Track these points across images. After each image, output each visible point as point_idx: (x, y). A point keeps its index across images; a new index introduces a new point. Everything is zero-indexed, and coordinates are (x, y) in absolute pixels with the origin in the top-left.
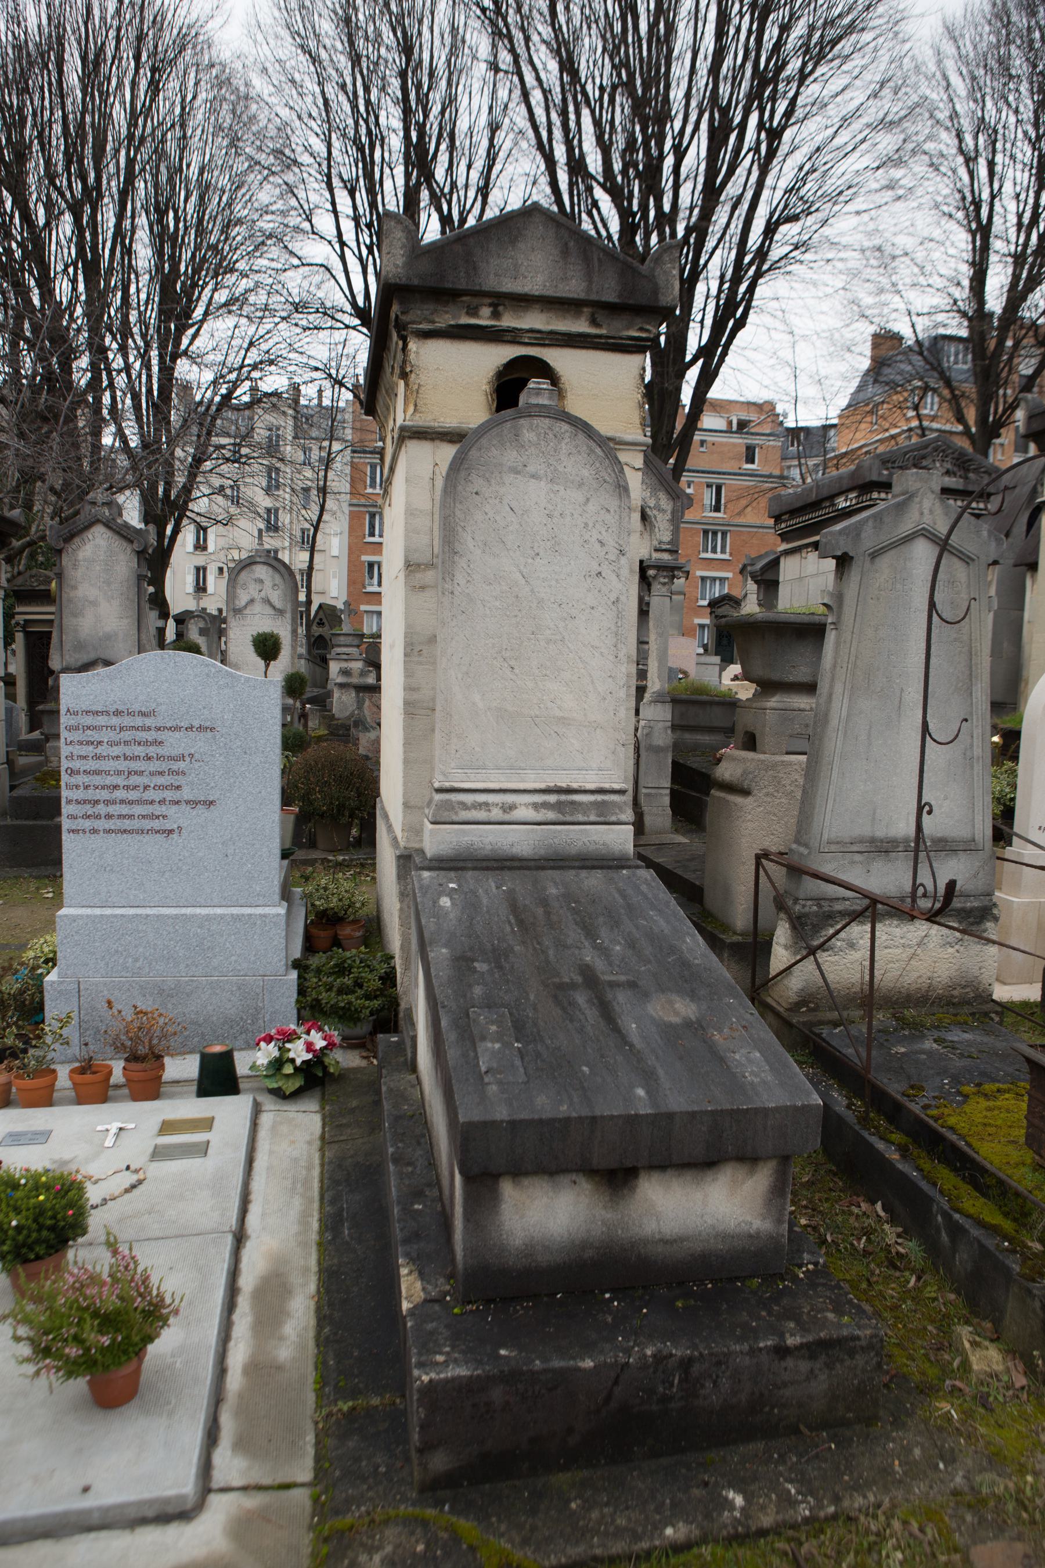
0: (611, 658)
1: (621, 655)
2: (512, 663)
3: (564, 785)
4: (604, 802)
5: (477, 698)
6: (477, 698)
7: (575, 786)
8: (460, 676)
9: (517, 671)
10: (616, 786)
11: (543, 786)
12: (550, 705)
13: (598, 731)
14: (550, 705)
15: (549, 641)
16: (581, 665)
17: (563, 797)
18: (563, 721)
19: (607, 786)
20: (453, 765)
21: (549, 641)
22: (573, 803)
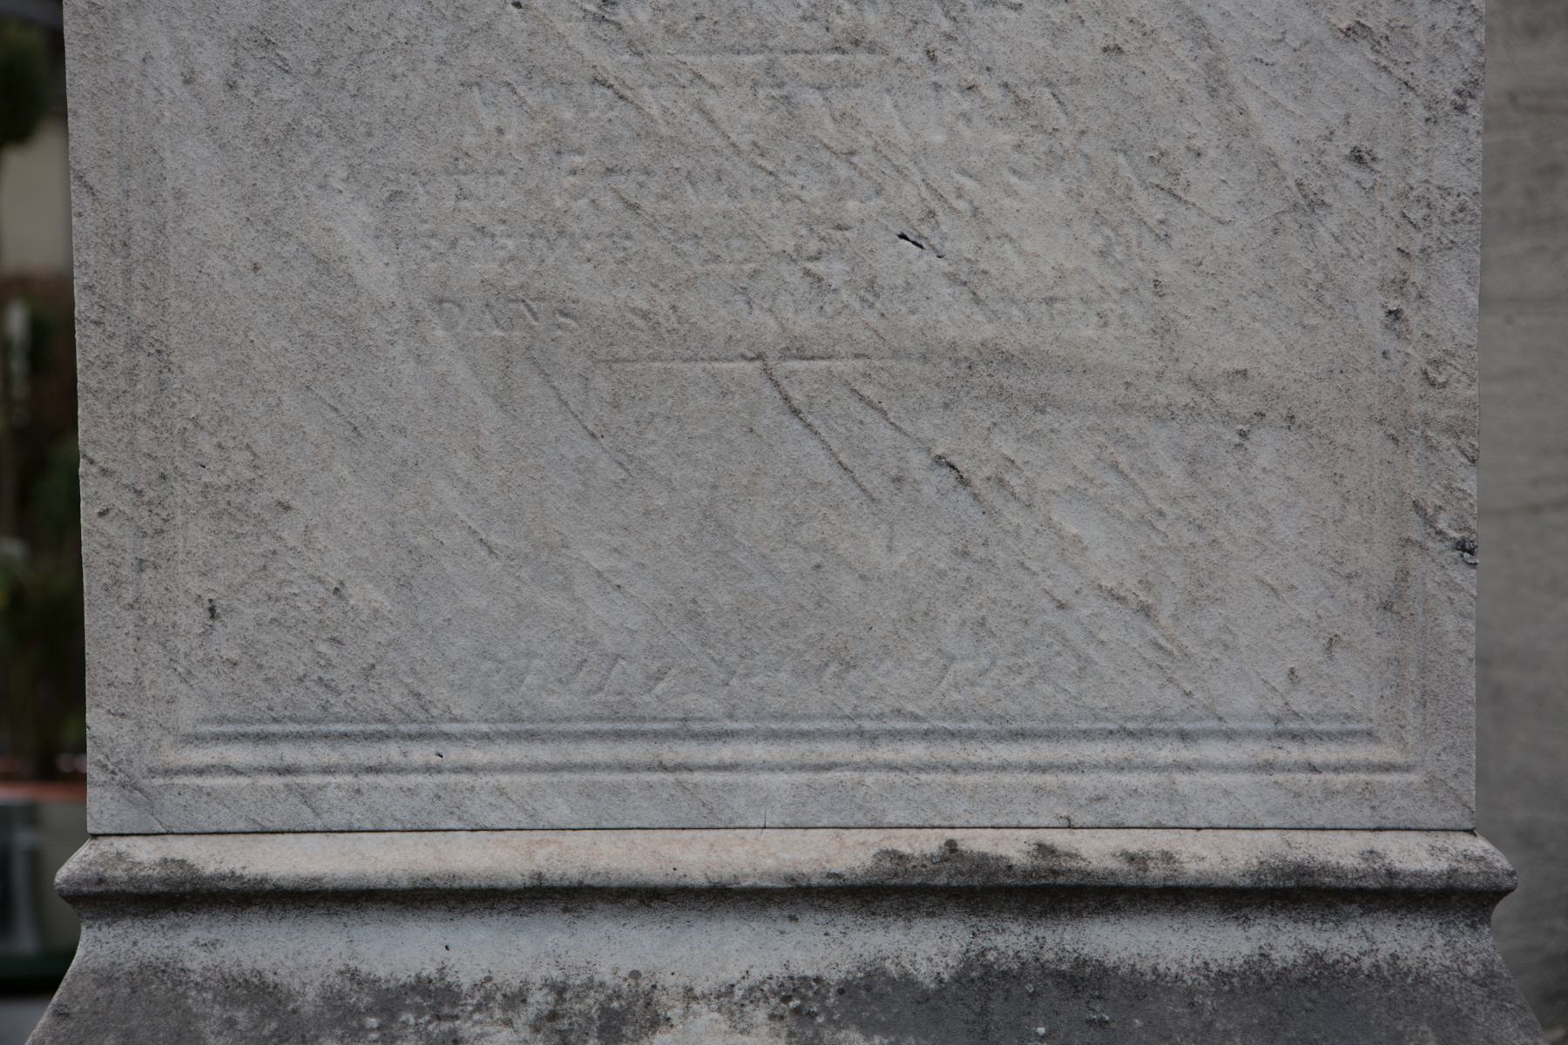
3: (1013, 848)
4: (1322, 977)
5: (349, 223)
6: (349, 223)
7: (1097, 851)
8: (212, 61)
10: (1414, 856)
11: (851, 855)
12: (892, 260)
13: (1267, 446)
17: (1012, 940)
18: (998, 377)
19: (1342, 852)
20: (188, 714)
22: (1084, 980)
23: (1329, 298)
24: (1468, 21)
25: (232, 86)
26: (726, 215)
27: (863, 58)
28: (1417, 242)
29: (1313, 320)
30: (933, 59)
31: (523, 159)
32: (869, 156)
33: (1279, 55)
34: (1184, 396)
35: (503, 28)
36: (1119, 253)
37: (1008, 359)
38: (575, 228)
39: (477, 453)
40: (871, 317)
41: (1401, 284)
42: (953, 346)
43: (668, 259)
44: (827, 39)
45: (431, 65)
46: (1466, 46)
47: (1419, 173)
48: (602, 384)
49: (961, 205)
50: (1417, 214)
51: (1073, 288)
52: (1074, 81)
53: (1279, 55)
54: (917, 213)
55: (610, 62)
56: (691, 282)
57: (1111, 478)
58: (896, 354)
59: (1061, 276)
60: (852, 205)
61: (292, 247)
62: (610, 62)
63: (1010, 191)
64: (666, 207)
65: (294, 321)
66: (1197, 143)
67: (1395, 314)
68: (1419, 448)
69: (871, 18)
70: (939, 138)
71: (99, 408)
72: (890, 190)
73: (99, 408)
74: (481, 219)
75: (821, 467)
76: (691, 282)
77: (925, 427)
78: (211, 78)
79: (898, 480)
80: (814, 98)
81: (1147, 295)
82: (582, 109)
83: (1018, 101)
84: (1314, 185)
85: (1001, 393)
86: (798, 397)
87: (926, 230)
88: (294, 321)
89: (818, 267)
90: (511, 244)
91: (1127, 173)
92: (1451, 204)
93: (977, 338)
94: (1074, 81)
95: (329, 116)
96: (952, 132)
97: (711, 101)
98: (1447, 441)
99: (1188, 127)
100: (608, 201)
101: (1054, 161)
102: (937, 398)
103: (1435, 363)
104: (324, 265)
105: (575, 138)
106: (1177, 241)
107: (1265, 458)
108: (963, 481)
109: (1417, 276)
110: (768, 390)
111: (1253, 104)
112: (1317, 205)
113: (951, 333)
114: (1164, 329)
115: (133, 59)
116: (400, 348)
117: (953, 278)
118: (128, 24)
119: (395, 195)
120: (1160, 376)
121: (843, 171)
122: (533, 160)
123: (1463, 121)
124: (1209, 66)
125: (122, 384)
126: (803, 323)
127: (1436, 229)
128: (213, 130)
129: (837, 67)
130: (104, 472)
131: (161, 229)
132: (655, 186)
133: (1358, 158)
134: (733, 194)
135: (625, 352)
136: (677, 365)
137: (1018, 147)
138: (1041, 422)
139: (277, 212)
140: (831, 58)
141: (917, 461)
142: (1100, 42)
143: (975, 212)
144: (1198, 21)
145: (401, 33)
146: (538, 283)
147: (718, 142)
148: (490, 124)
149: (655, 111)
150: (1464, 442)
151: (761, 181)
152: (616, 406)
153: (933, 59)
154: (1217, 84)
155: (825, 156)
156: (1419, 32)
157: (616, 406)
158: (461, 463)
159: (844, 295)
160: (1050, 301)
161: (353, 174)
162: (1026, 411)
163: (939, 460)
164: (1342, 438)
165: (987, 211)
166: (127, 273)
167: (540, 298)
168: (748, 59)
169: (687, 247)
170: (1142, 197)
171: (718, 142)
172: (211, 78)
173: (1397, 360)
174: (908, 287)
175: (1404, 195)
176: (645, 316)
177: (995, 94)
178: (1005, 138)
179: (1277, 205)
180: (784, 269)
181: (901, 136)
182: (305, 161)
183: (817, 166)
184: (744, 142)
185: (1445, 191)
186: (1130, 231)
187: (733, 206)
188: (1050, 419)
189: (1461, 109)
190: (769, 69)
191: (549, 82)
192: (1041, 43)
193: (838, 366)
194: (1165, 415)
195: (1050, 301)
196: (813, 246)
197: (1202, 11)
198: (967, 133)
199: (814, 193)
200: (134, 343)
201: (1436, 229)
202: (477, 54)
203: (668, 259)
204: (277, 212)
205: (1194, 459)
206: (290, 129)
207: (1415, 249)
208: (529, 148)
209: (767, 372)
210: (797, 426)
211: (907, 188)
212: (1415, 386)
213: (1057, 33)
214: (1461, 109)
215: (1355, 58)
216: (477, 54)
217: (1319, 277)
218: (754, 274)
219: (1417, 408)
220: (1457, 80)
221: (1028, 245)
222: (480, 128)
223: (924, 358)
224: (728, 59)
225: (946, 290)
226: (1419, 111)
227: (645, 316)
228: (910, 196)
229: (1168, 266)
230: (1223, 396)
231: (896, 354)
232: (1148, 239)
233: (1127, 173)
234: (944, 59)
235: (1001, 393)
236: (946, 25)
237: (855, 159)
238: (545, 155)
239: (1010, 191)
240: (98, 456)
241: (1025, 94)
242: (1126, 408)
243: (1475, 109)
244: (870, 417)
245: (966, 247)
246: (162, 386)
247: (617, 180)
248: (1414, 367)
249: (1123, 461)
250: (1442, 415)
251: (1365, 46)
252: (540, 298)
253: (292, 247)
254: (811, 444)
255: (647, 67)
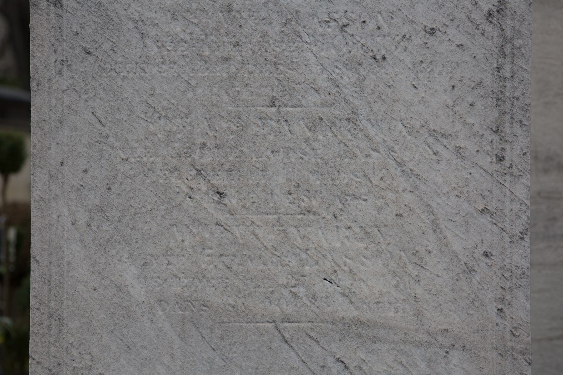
0: (486, 161)
1: (512, 154)
2: (221, 180)
5: (128, 273)
6: (128, 273)
8: (82, 217)
9: (232, 201)
12: (321, 287)
13: (456, 356)
14: (321, 287)
15: (314, 124)
16: (402, 183)
18: (358, 330)
21: (314, 124)
23: (477, 304)
24: (524, 208)
25: (89, 226)
26: (263, 271)
27: (311, 217)
28: (508, 285)
29: (471, 312)
30: (336, 217)
31: (191, 251)
32: (313, 251)
33: (458, 218)
34: (426, 338)
35: (185, 206)
36: (402, 286)
37: (362, 323)
38: (209, 275)
39: (172, 355)
40: (314, 308)
41: (502, 300)
42: (343, 319)
43: (241, 286)
44: (299, 210)
45: (159, 218)
46: (524, 217)
47: (508, 261)
48: (217, 331)
49: (346, 269)
50: (507, 275)
51: (386, 299)
52: (386, 226)
53: (458, 218)
54: (330, 271)
55: (222, 217)
56: (249, 295)
57: (399, 367)
58: (322, 321)
59: (381, 294)
60: (307, 268)
61: (108, 282)
62: (222, 217)
63: (363, 264)
64: (241, 268)
65: (108, 308)
66: (429, 248)
67: (500, 310)
68: (510, 359)
69: (314, 203)
70: (338, 245)
71: (37, 339)
72: (321, 263)
73: (37, 339)
74: (175, 272)
75: (295, 362)
76: (249, 295)
77: (333, 347)
78: (82, 223)
79: (323, 367)
80: (294, 230)
81: (412, 301)
82: (212, 233)
83: (366, 233)
84: (471, 264)
85: (360, 336)
86: (287, 336)
87: (333, 277)
88: (108, 308)
89: (295, 290)
90: (186, 281)
91: (404, 258)
92: (520, 272)
93: (351, 316)
94: (386, 226)
95: (123, 236)
96: (342, 243)
97: (258, 231)
98: (520, 356)
99: (426, 243)
100: (221, 266)
101: (379, 254)
102: (337, 337)
103: (515, 328)
104: (119, 288)
105: (209, 243)
106: (423, 282)
107: (454, 361)
108: (346, 367)
109: (508, 297)
110: (277, 333)
111: (449, 235)
112: (472, 271)
113: (342, 314)
114: (418, 314)
115: (55, 216)
116: (145, 318)
117: (343, 294)
118: (53, 204)
119: (145, 263)
120: (417, 331)
121: (304, 256)
122: (194, 251)
123: (523, 243)
124: (433, 222)
125: (46, 331)
126: (290, 310)
127: (514, 280)
128: (81, 241)
129: (302, 220)
130: (38, 363)
131: (62, 276)
132: (237, 261)
133: (486, 255)
134: (265, 264)
135: (226, 319)
136: (244, 325)
137: (366, 248)
138: (375, 346)
139: (103, 269)
140: (300, 217)
141: (330, 360)
142: (395, 213)
143: (351, 271)
144: (429, 206)
145: (149, 207)
146: (195, 295)
147: (260, 245)
148: (179, 239)
149: (238, 234)
150: (526, 357)
151: (275, 259)
152: (222, 339)
153: (336, 217)
154: (436, 228)
155: (298, 251)
156: (507, 211)
157: (222, 339)
158: (166, 359)
159: (304, 300)
160: (377, 303)
161: (130, 256)
162: (369, 343)
163: (338, 360)
164: (483, 354)
165: (355, 271)
166: (49, 291)
167: (196, 300)
168: (271, 217)
169: (248, 282)
170: (410, 267)
171: (260, 245)
172: (82, 223)
173: (502, 326)
174: (327, 297)
175: (502, 268)
176: (233, 306)
177: (358, 230)
178: (361, 245)
179: (458, 270)
180: (283, 290)
181: (325, 244)
182: (114, 252)
183: (295, 254)
184: (269, 245)
185: (517, 267)
186: (406, 279)
187: (265, 268)
188: (378, 345)
189: (522, 239)
190: (278, 220)
191: (201, 224)
192: (374, 213)
193: (302, 325)
194: (419, 345)
195: (377, 303)
196: (293, 282)
197: (431, 203)
198: (348, 243)
199: (294, 264)
200: (51, 316)
201: (514, 280)
202: (175, 215)
203: (241, 286)
204: (103, 269)
205: (429, 361)
206: (109, 240)
207: (507, 287)
208: (193, 247)
209: (276, 327)
210: (287, 346)
211: (327, 262)
212: (508, 336)
213: (380, 209)
214: (522, 239)
215: (484, 220)
216: (175, 215)
217: (473, 296)
218: (272, 292)
219: (509, 344)
220: (521, 228)
221: (369, 283)
222: (176, 240)
223: (333, 323)
224: (264, 217)
225: (340, 299)
226: (507, 239)
227: (233, 306)
228: (328, 265)
229: (419, 291)
230: (440, 338)
231: (322, 321)
232: (412, 282)
233: (404, 258)
234: (340, 218)
235: (360, 336)
236: (340, 206)
237: (308, 252)
238: (199, 250)
239: (363, 264)
240: (36, 357)
241: (369, 230)
242: (405, 342)
243: (527, 238)
244: (313, 344)
245: (347, 283)
246: (60, 331)
247: (224, 259)
248: (508, 329)
249: (404, 361)
250: (518, 347)
251: (488, 216)
252: (196, 300)
253: (108, 282)
254: (292, 353)
255: (235, 219)
